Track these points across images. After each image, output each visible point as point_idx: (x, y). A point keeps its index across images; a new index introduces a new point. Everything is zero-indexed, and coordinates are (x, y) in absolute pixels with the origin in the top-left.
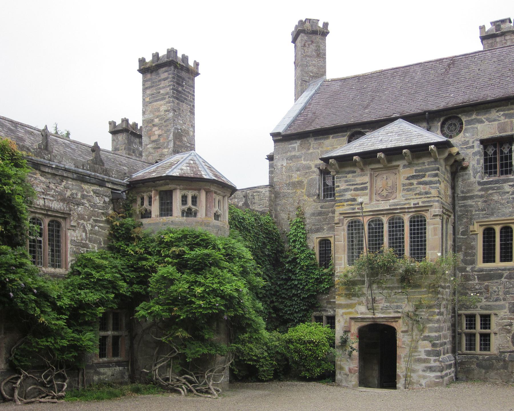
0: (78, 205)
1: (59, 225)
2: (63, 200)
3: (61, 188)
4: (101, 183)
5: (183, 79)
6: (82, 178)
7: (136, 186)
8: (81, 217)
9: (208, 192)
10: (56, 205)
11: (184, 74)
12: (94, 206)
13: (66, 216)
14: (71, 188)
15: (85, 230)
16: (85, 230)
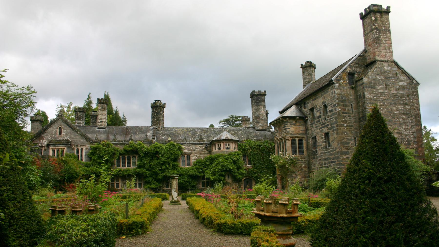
0: (195, 150)
1: (190, 156)
2: (190, 150)
3: (189, 148)
4: (202, 144)
5: (260, 98)
6: (195, 144)
7: (212, 143)
8: (195, 153)
9: (223, 143)
10: (188, 152)
11: (259, 96)
12: (200, 150)
13: (191, 153)
14: (192, 147)
15: (197, 156)
16: (197, 156)
